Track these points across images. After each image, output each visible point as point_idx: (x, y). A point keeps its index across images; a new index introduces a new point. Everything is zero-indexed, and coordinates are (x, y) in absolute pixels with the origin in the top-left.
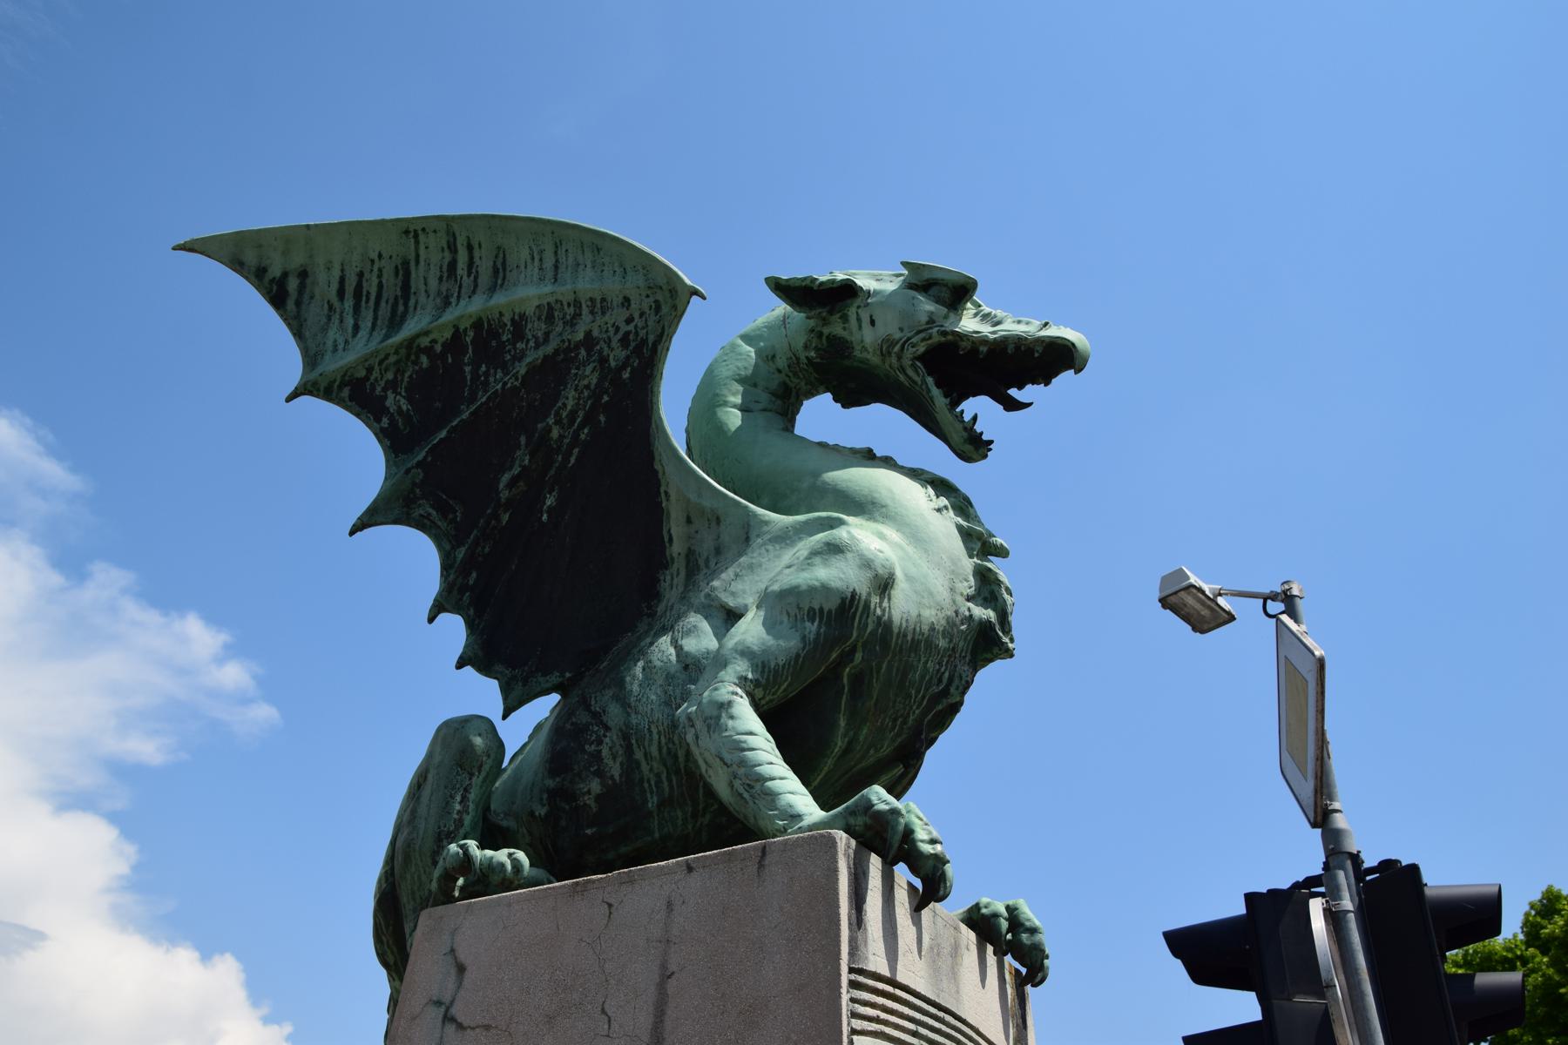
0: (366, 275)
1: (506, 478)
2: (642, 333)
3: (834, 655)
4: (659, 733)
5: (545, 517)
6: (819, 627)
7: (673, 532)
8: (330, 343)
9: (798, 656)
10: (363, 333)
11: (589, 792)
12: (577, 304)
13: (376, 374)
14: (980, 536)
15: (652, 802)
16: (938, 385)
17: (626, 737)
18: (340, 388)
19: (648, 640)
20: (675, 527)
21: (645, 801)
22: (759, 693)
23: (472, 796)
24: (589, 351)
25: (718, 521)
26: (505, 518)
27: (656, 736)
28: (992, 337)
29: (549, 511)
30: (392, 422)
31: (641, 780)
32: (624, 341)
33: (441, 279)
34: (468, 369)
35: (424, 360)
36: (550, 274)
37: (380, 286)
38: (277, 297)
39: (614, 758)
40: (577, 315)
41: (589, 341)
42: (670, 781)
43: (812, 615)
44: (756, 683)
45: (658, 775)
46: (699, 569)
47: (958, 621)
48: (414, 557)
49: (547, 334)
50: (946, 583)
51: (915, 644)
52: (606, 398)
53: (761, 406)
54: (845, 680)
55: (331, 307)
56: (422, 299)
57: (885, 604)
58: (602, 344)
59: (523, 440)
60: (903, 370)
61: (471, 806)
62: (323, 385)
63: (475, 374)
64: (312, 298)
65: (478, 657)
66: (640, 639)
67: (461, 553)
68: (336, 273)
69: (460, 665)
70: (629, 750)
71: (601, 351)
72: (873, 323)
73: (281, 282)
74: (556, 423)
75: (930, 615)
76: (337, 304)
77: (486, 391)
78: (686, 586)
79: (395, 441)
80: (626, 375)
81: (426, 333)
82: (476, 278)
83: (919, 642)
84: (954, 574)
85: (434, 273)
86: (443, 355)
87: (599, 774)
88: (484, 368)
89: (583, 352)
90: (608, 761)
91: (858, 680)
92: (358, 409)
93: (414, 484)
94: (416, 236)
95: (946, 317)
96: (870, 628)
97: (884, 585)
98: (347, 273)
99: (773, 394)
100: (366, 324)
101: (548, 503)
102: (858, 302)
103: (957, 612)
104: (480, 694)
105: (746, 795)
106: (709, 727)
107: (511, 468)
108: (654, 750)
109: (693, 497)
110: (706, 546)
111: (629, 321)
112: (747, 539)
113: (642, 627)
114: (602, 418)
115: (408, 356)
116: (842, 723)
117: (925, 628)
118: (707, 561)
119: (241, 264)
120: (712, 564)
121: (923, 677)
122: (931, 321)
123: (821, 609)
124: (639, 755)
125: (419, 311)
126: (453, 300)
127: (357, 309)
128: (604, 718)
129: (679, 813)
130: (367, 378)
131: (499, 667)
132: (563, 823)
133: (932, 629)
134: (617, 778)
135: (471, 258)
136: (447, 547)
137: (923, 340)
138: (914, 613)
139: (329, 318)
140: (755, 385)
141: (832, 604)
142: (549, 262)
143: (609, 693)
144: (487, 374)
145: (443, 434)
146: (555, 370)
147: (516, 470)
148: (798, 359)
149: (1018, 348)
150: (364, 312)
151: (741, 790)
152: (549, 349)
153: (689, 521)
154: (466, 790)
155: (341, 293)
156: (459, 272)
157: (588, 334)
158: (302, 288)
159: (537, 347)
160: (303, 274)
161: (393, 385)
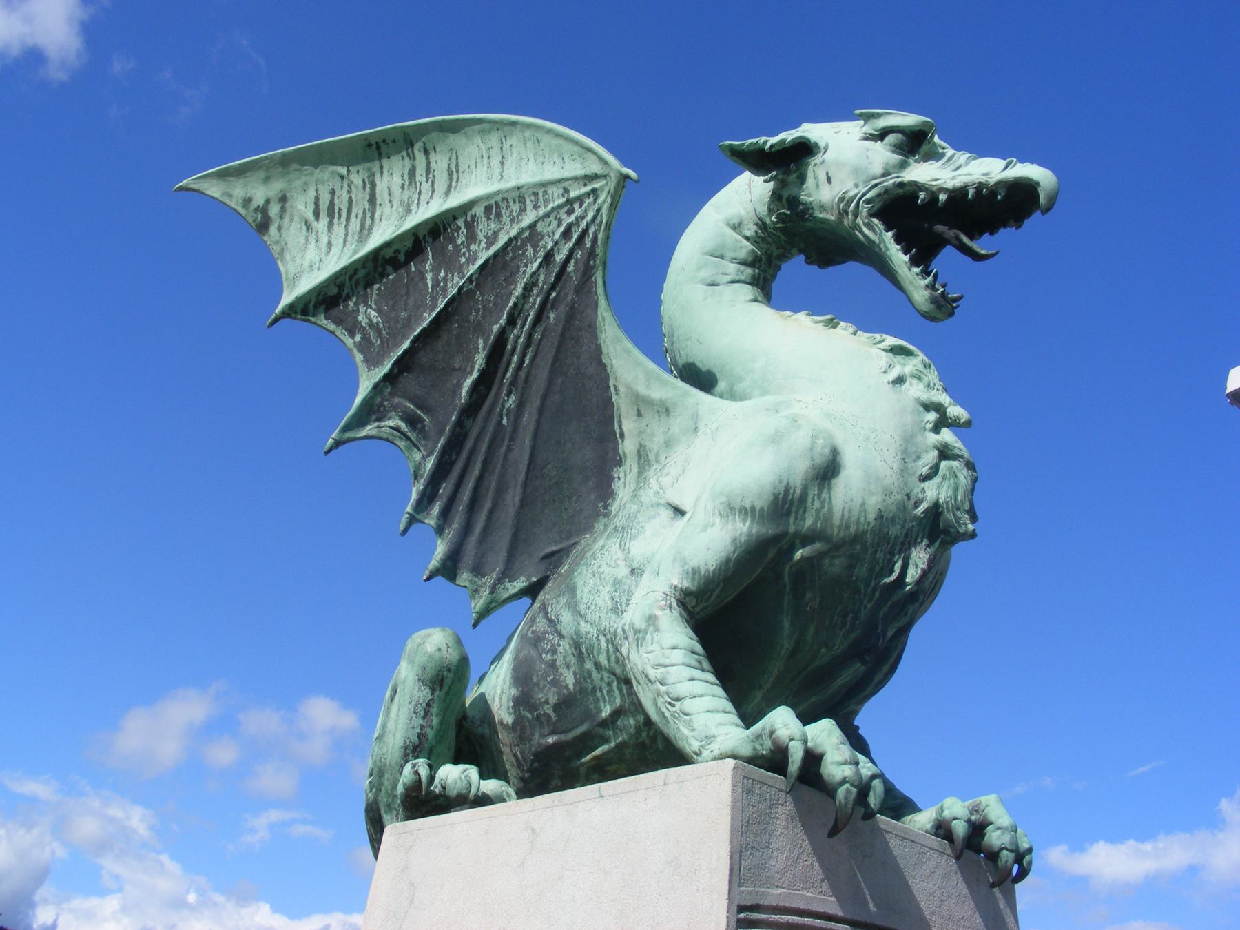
0: (338, 193)
1: (468, 383)
2: (583, 224)
3: (771, 554)
4: (607, 641)
5: (505, 421)
6: (750, 527)
7: (624, 428)
8: (306, 263)
9: (728, 560)
10: (335, 250)
11: (547, 702)
12: (522, 199)
13: (346, 291)
15: (606, 712)
16: (898, 240)
17: (576, 645)
18: (315, 307)
19: (601, 543)
20: (628, 425)
21: (599, 711)
22: (691, 602)
23: (434, 710)
24: (535, 247)
25: (667, 410)
27: (604, 645)
28: (950, 185)
29: (507, 415)
30: (366, 338)
31: (594, 690)
32: (567, 234)
33: (403, 187)
34: (429, 276)
36: (497, 171)
37: (350, 201)
39: (568, 666)
40: (523, 210)
42: (620, 690)
43: (745, 512)
45: (609, 684)
46: (649, 465)
47: (911, 504)
49: (496, 234)
50: (896, 466)
51: (858, 538)
52: (554, 294)
53: (729, 278)
54: (786, 579)
55: (308, 227)
56: (387, 209)
57: (825, 495)
59: (481, 342)
60: (861, 231)
61: (435, 721)
63: (436, 283)
64: (292, 220)
66: (595, 541)
67: (430, 464)
68: (312, 193)
70: (580, 657)
71: (545, 247)
72: (829, 180)
73: (264, 210)
74: (511, 321)
75: (874, 503)
76: (314, 224)
77: (444, 297)
78: (638, 483)
80: (570, 268)
81: (387, 245)
82: (433, 183)
83: (864, 533)
84: (908, 454)
85: (397, 180)
87: (555, 683)
88: (442, 274)
89: (530, 249)
90: (563, 671)
92: (332, 327)
94: (378, 148)
95: (903, 166)
96: (809, 522)
98: (321, 192)
101: (507, 405)
103: (908, 496)
105: (667, 714)
106: (637, 640)
107: (471, 373)
108: (603, 660)
109: (641, 389)
110: (654, 444)
112: (696, 429)
113: (599, 526)
114: (552, 316)
115: (375, 268)
116: (786, 624)
117: (871, 516)
118: (657, 455)
119: (230, 196)
120: (662, 458)
121: (871, 570)
122: (886, 174)
123: (753, 509)
124: (589, 665)
125: (384, 222)
126: (413, 208)
127: (330, 225)
128: (558, 627)
129: (632, 721)
132: (528, 731)
133: (880, 516)
134: (571, 686)
135: (428, 163)
137: (879, 195)
138: (858, 501)
139: (307, 240)
140: (722, 257)
141: (762, 503)
142: (495, 162)
143: (563, 600)
144: (445, 279)
145: (406, 345)
147: (475, 375)
148: (764, 223)
150: (335, 227)
151: (664, 710)
153: (639, 414)
154: (428, 705)
155: (317, 214)
156: (418, 178)
157: (532, 226)
159: (487, 248)
160: (283, 199)
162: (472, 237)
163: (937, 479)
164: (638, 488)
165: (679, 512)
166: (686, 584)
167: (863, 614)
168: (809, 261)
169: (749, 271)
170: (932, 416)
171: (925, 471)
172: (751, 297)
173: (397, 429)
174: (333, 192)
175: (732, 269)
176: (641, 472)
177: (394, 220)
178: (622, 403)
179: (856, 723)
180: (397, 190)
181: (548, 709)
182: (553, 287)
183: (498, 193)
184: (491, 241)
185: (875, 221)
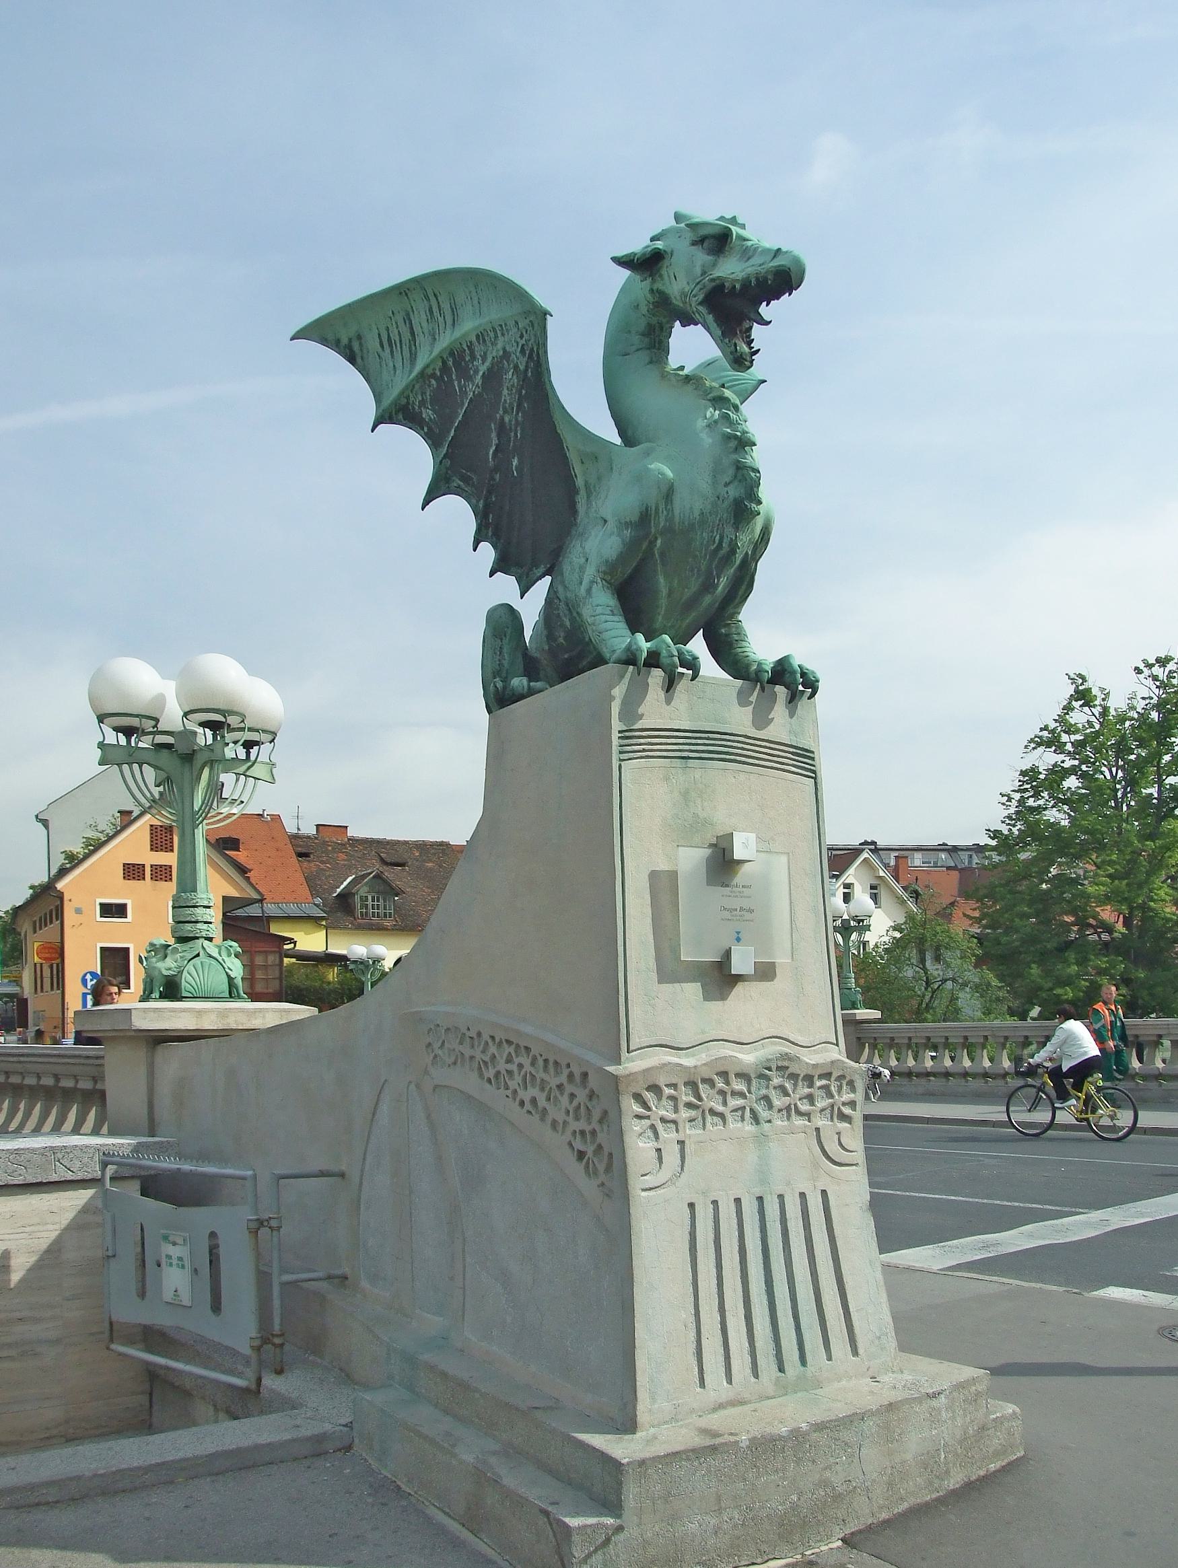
3: (644, 547)
13: (412, 399)
14: (736, 437)
20: (578, 469)
23: (505, 650)
26: (497, 477)
28: (740, 277)
30: (430, 429)
32: (523, 351)
35: (433, 382)
38: (352, 359)
40: (496, 337)
41: (506, 355)
43: (628, 524)
44: (605, 573)
48: (457, 513)
49: (485, 354)
51: (692, 527)
53: (634, 348)
58: (513, 356)
62: (387, 416)
65: (501, 565)
67: (481, 504)
69: (491, 574)
74: (505, 411)
75: (698, 505)
76: (382, 354)
79: (433, 440)
81: (428, 366)
83: (693, 524)
84: (716, 473)
86: (441, 376)
87: (562, 625)
91: (663, 554)
93: (447, 469)
95: (714, 265)
97: (669, 493)
99: (643, 335)
100: (399, 364)
101: (515, 462)
102: (666, 262)
104: (506, 588)
111: (522, 337)
116: (662, 580)
117: (697, 513)
122: (704, 273)
124: (575, 614)
127: (392, 352)
130: (408, 403)
131: (513, 569)
136: (474, 501)
141: (635, 517)
142: (476, 302)
146: (493, 377)
149: (757, 279)
152: (488, 364)
158: (361, 344)
160: (359, 337)
161: (423, 403)
162: (473, 358)
163: (736, 483)
164: (588, 508)
165: (605, 521)
166: (604, 568)
167: (703, 568)
168: (683, 325)
169: (647, 340)
170: (733, 444)
171: (727, 480)
172: (647, 359)
173: (459, 487)
174: (388, 329)
175: (636, 339)
176: (588, 497)
177: (428, 348)
178: (573, 457)
179: (740, 617)
180: (425, 324)
181: (561, 640)
182: (522, 388)
183: (480, 325)
184: (484, 359)
185: (701, 308)
